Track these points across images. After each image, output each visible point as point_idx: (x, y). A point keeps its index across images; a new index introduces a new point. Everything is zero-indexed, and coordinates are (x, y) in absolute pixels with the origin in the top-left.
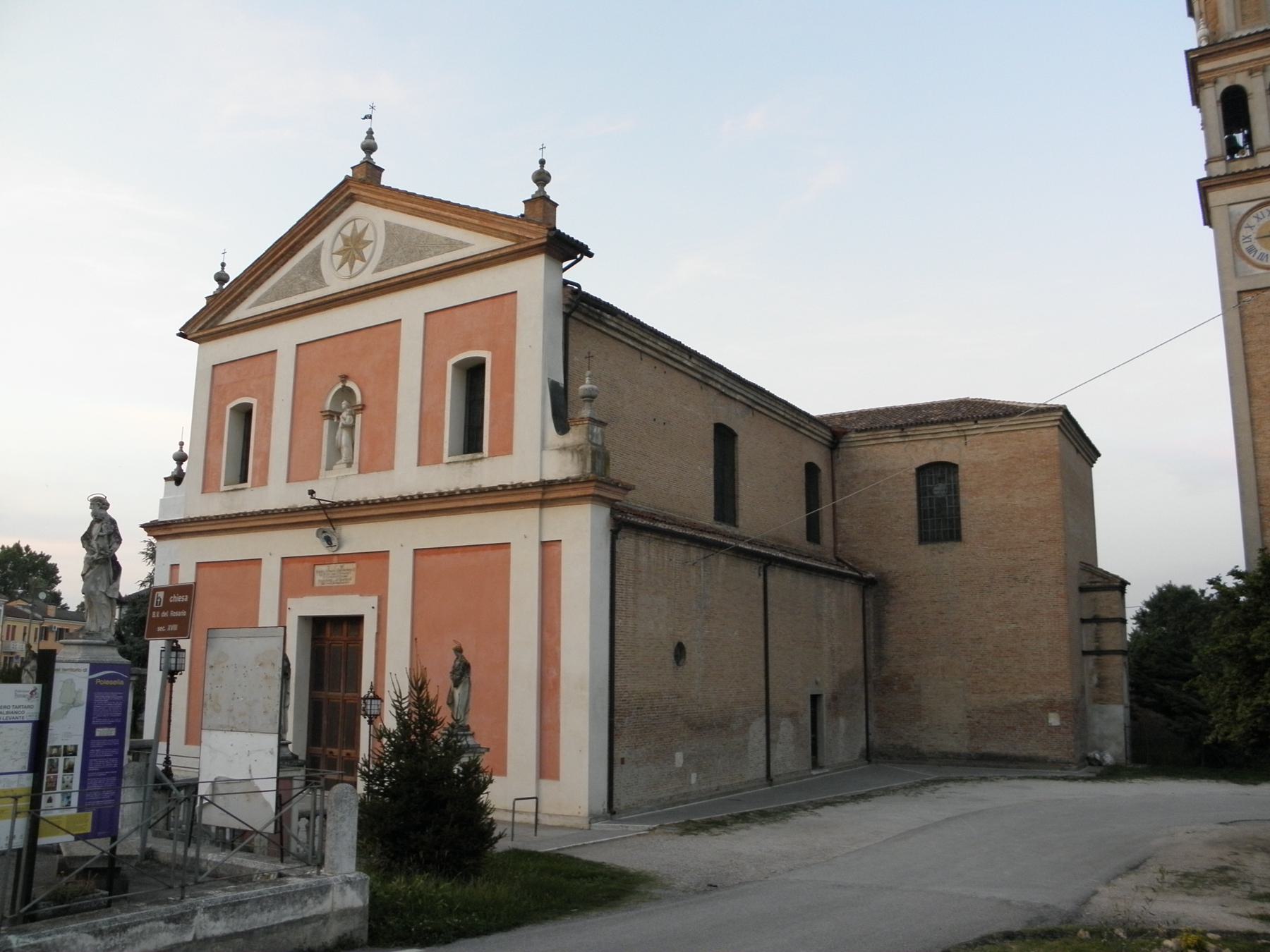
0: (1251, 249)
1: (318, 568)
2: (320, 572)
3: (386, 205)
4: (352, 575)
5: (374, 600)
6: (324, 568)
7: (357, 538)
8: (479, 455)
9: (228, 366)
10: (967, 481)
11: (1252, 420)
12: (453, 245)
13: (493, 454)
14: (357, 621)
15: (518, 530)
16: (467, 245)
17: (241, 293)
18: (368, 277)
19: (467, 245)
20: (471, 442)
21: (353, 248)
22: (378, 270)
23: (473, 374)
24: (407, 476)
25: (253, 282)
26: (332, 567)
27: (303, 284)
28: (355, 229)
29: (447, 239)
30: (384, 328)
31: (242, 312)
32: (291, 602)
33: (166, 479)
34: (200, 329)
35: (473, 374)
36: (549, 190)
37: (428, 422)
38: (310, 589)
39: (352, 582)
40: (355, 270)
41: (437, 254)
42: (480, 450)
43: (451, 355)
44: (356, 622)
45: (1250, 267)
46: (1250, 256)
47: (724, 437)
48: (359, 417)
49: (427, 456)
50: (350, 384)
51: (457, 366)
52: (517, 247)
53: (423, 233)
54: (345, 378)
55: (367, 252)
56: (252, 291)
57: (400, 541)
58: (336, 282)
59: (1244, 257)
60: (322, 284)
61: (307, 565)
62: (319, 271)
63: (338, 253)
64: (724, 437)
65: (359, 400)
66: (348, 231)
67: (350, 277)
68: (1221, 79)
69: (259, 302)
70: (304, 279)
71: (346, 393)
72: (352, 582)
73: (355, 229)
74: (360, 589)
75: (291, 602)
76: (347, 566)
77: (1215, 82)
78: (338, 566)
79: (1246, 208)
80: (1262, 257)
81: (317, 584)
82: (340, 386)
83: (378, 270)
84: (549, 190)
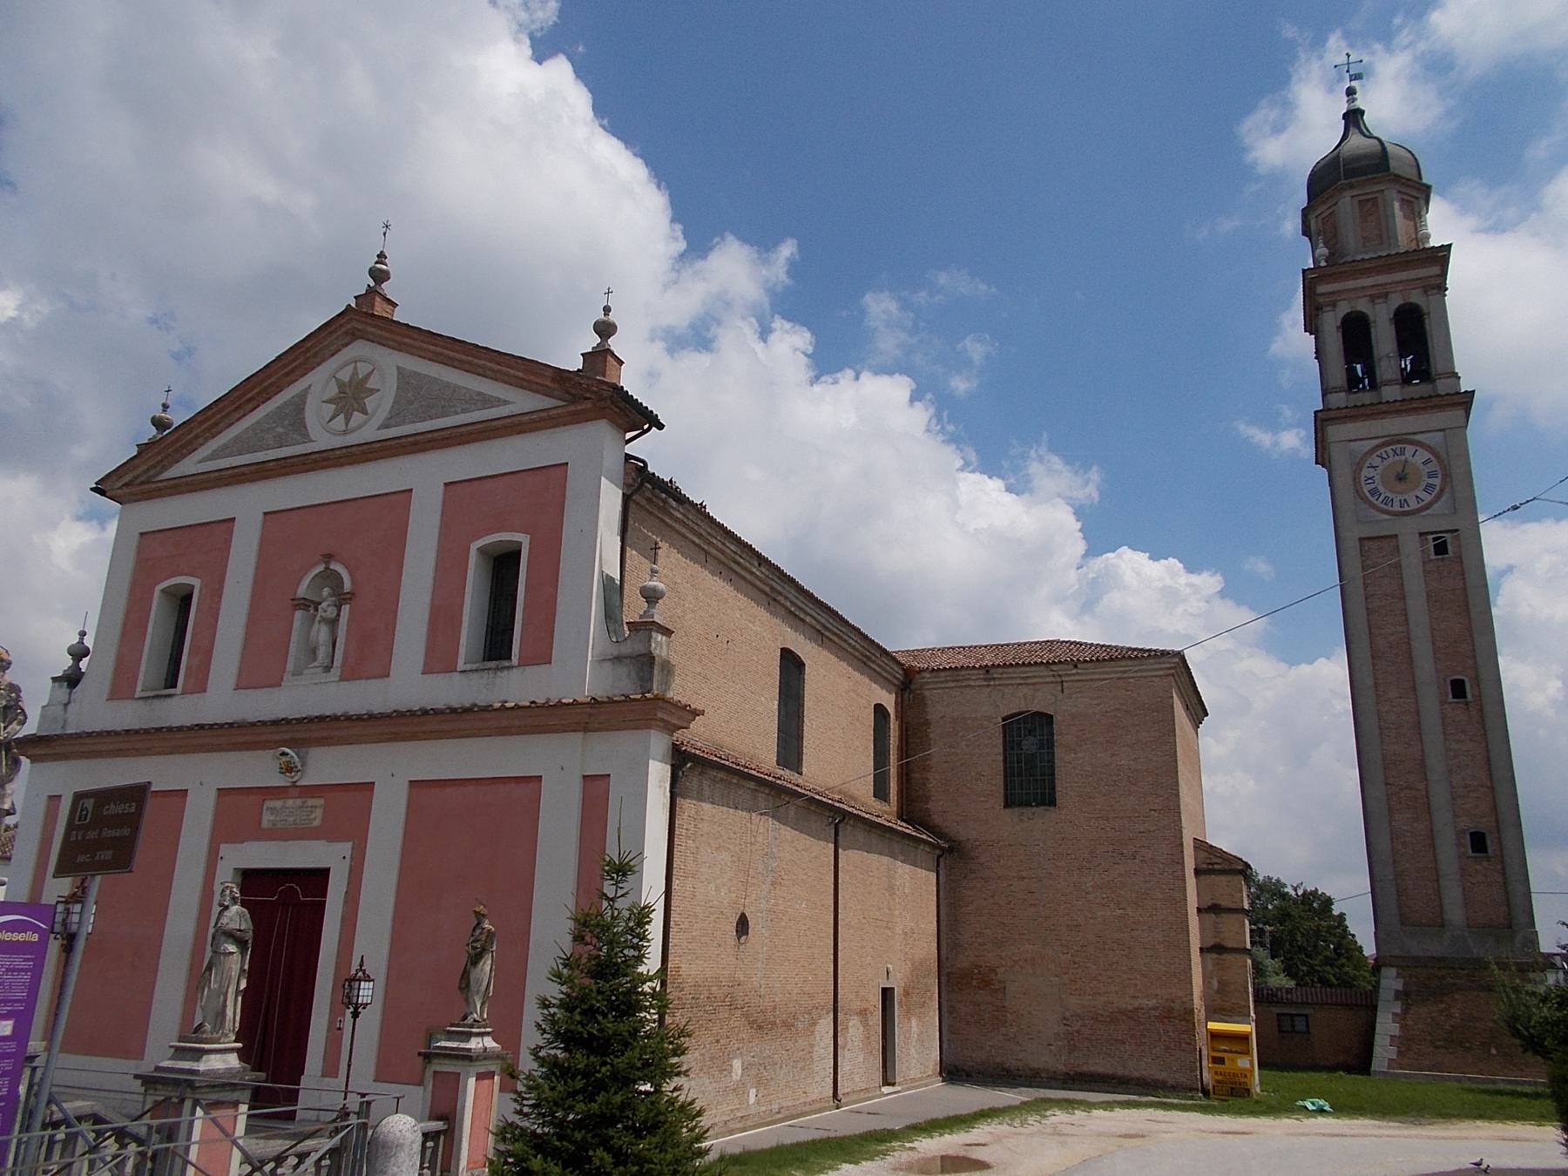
0: (1374, 492)
1: (268, 804)
2: (272, 810)
3: (400, 347)
4: (318, 813)
5: (346, 848)
6: (278, 804)
7: (328, 766)
8: (506, 663)
9: (161, 535)
10: (1063, 734)
11: (1376, 685)
12: (487, 401)
13: (525, 662)
14: (317, 879)
15: (556, 763)
16: (506, 402)
17: (190, 442)
18: (369, 432)
19: (506, 402)
20: (496, 647)
21: (351, 397)
22: (385, 426)
23: (503, 565)
24: (408, 683)
25: (208, 429)
26: (290, 803)
28: (355, 373)
29: (479, 394)
31: (188, 466)
32: (224, 849)
33: (55, 679)
35: (503, 565)
36: (614, 343)
37: (442, 619)
39: (317, 823)
40: (352, 424)
41: (464, 411)
42: (509, 658)
44: (317, 879)
45: (1374, 512)
46: (1373, 500)
47: (791, 664)
48: (346, 609)
49: (439, 660)
50: (336, 566)
51: (481, 550)
52: (572, 408)
53: (448, 385)
54: (328, 557)
55: (370, 402)
57: (391, 771)
58: (322, 439)
59: (1364, 499)
60: (306, 438)
62: (303, 421)
63: (330, 401)
64: (791, 664)
65: (347, 586)
66: (345, 375)
67: (345, 432)
69: (213, 456)
70: (280, 430)
73: (355, 373)
74: (328, 832)
75: (224, 849)
76: (310, 802)
78: (299, 802)
80: (1386, 501)
81: (265, 824)
82: (321, 568)
83: (385, 426)
84: (614, 343)
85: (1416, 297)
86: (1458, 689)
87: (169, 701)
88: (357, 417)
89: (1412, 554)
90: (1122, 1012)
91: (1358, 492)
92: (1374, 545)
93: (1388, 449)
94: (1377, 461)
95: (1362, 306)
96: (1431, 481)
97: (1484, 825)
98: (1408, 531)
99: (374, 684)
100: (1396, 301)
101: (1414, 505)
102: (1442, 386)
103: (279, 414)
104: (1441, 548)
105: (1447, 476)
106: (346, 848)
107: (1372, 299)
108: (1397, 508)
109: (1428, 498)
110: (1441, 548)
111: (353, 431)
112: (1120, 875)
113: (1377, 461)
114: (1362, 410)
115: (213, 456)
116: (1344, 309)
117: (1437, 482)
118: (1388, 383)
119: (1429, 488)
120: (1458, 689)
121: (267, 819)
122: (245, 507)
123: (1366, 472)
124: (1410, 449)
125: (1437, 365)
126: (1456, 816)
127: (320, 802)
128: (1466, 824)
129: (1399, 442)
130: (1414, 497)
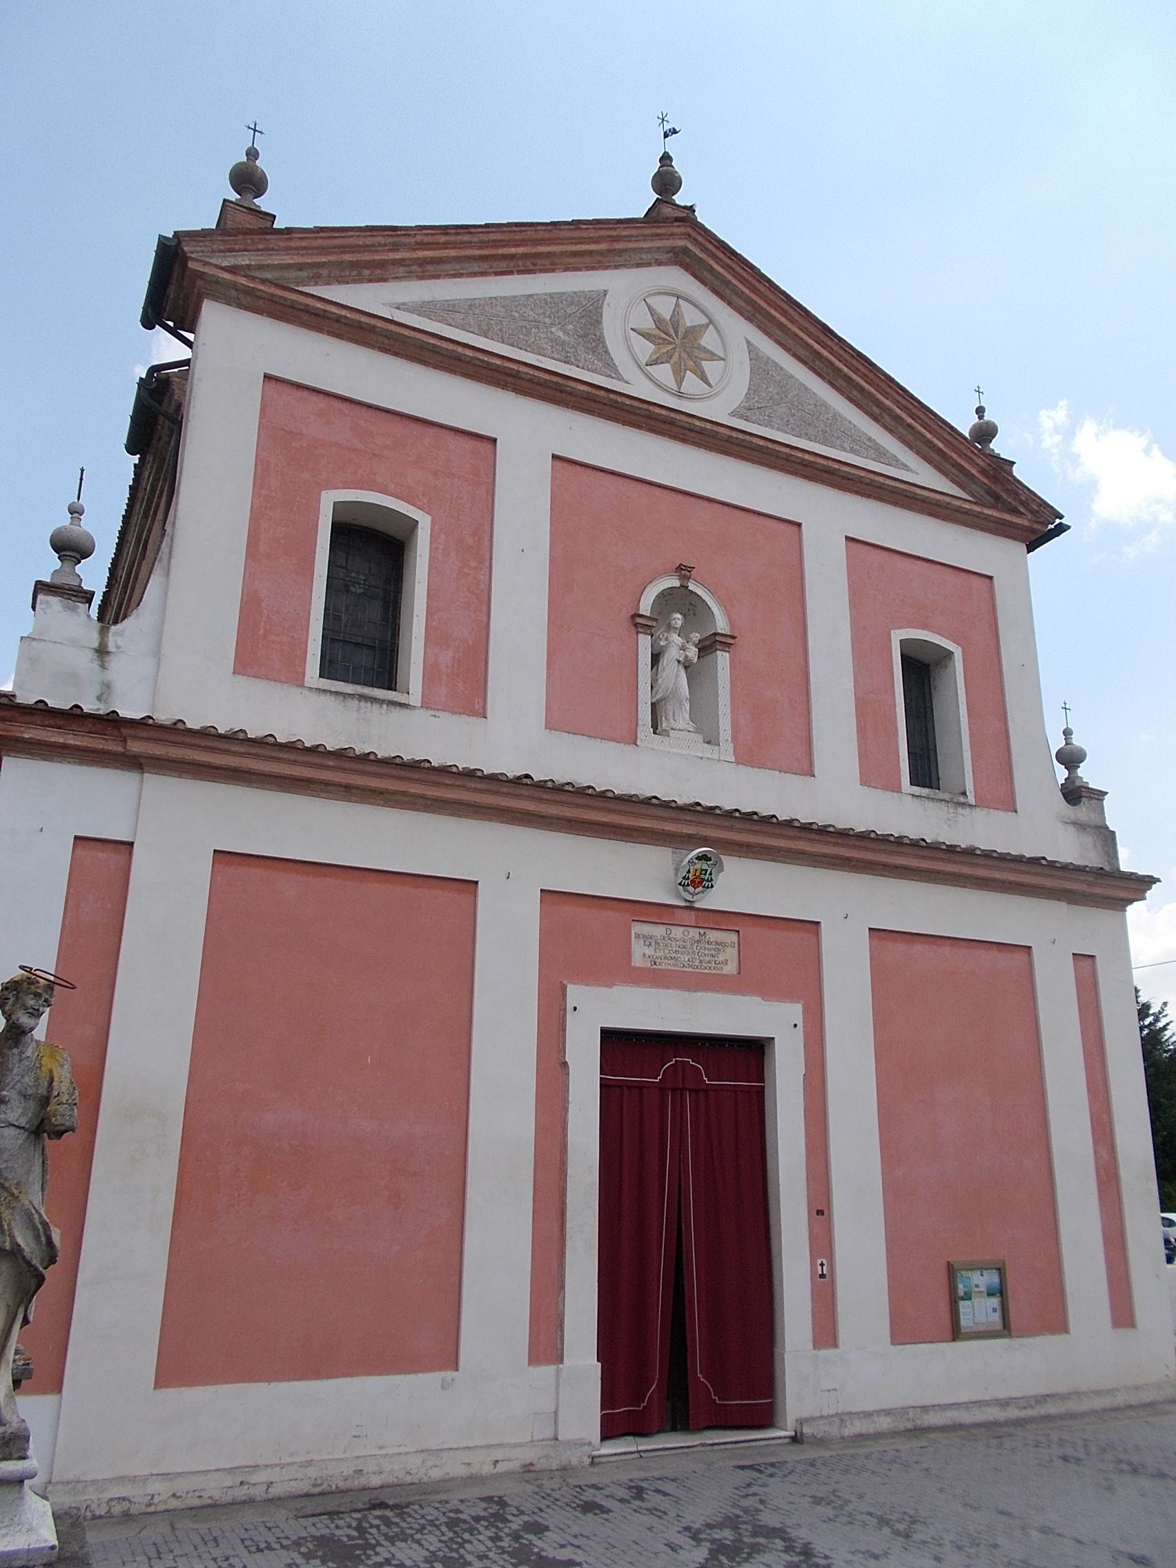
1: (637, 928)
4: (731, 954)
5: (794, 1012)
6: (658, 931)
7: (743, 885)
12: (881, 454)
14: (751, 1054)
17: (383, 264)
19: (905, 467)
23: (921, 670)
24: (837, 791)
25: (423, 262)
26: (677, 932)
27: (555, 341)
29: (869, 439)
30: (761, 520)
34: (232, 270)
35: (921, 670)
38: (614, 969)
41: (852, 450)
43: (910, 624)
44: (751, 1054)
53: (824, 404)
56: (409, 276)
57: (848, 912)
61: (611, 915)
62: (600, 340)
66: (665, 307)
71: (680, 601)
72: (731, 969)
75: (575, 994)
76: (713, 936)
78: (694, 933)
81: (638, 960)
87: (396, 713)
88: (691, 382)
99: (795, 783)
103: (553, 301)
106: (794, 1012)
111: (691, 398)
115: (422, 309)
121: (640, 954)
122: (529, 435)
127: (733, 937)
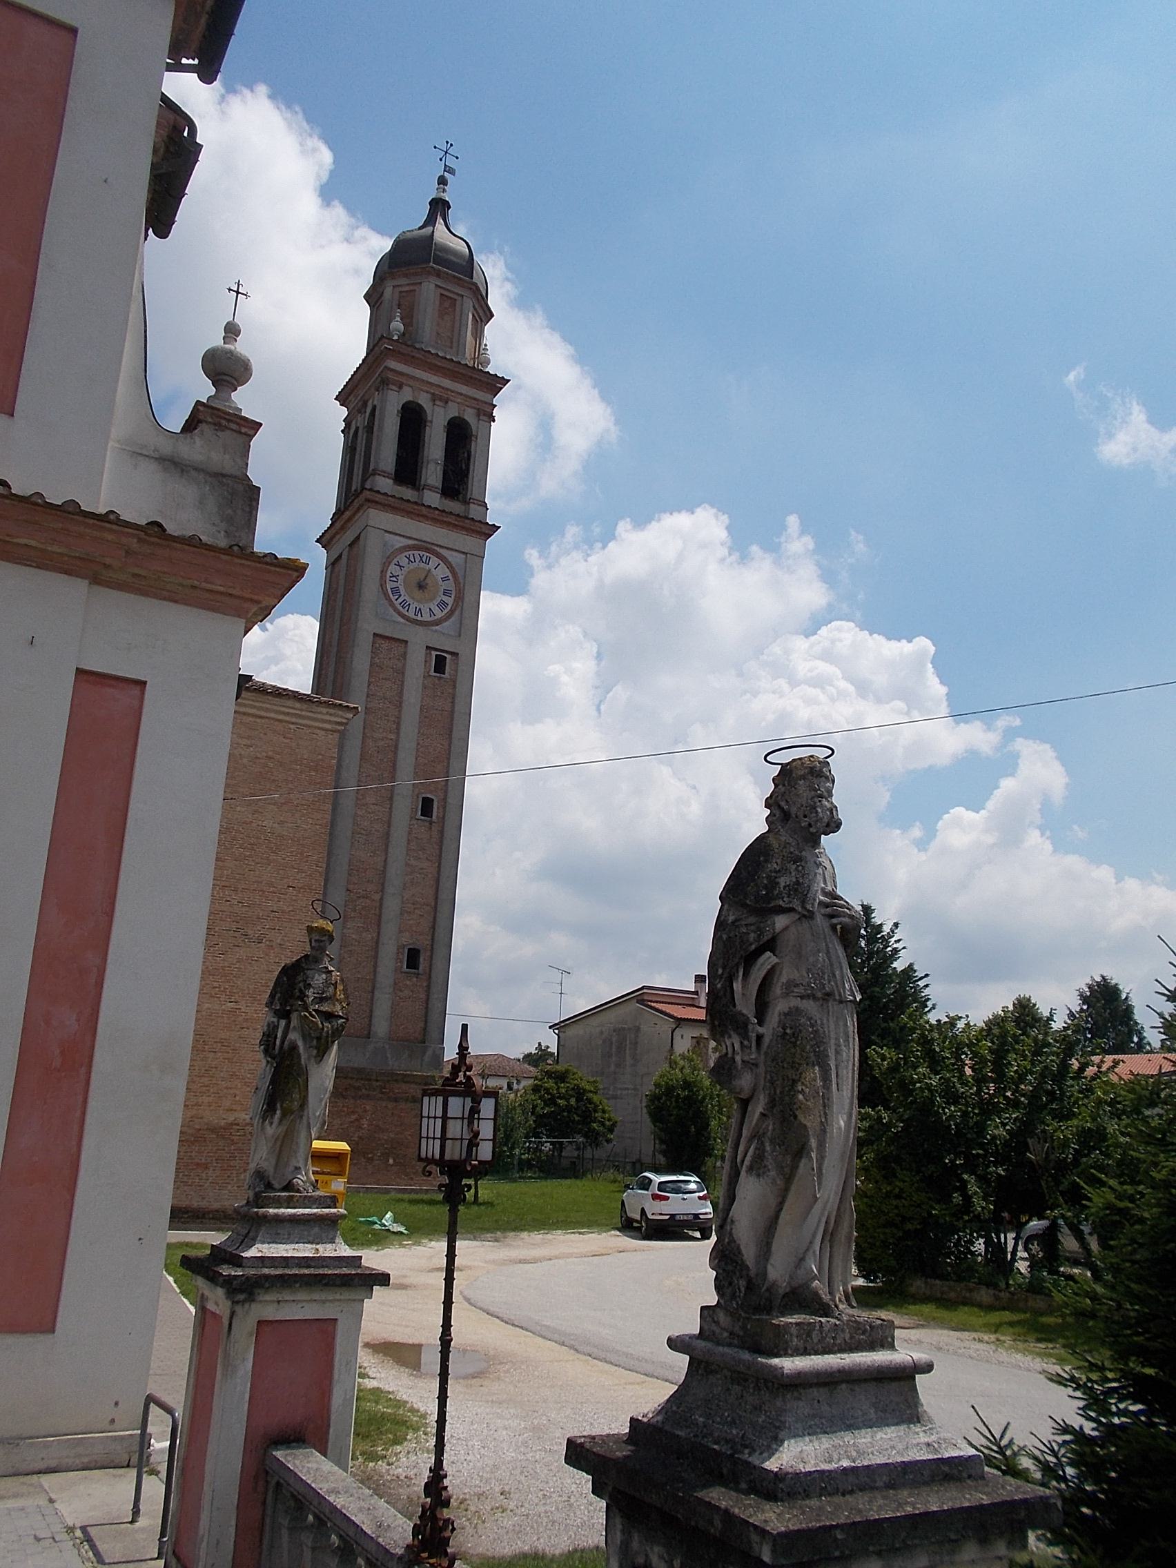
0: (395, 591)
45: (391, 610)
46: (393, 599)
68: (406, 388)
77: (400, 386)
79: (400, 542)
85: (469, 416)
86: (427, 807)
89: (417, 665)
90: (213, 1130)
91: (383, 586)
92: (385, 644)
93: (416, 553)
94: (404, 561)
95: (424, 400)
96: (445, 599)
97: (422, 942)
98: (419, 640)
100: (453, 411)
101: (426, 617)
102: (474, 511)
104: (440, 665)
105: (459, 598)
107: (434, 398)
108: (411, 614)
109: (439, 614)
110: (440, 665)
112: (239, 961)
113: (404, 561)
114: (405, 505)
116: (407, 395)
117: (450, 601)
118: (431, 488)
119: (442, 604)
120: (427, 807)
123: (393, 569)
124: (434, 560)
125: (474, 492)
126: (400, 932)
128: (406, 939)
129: (427, 550)
130: (430, 609)
